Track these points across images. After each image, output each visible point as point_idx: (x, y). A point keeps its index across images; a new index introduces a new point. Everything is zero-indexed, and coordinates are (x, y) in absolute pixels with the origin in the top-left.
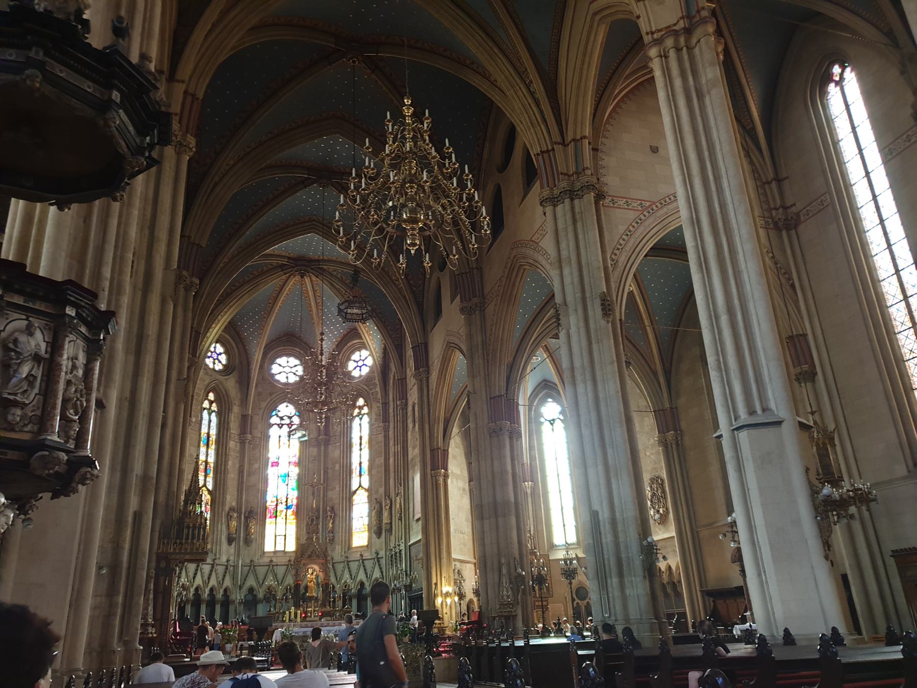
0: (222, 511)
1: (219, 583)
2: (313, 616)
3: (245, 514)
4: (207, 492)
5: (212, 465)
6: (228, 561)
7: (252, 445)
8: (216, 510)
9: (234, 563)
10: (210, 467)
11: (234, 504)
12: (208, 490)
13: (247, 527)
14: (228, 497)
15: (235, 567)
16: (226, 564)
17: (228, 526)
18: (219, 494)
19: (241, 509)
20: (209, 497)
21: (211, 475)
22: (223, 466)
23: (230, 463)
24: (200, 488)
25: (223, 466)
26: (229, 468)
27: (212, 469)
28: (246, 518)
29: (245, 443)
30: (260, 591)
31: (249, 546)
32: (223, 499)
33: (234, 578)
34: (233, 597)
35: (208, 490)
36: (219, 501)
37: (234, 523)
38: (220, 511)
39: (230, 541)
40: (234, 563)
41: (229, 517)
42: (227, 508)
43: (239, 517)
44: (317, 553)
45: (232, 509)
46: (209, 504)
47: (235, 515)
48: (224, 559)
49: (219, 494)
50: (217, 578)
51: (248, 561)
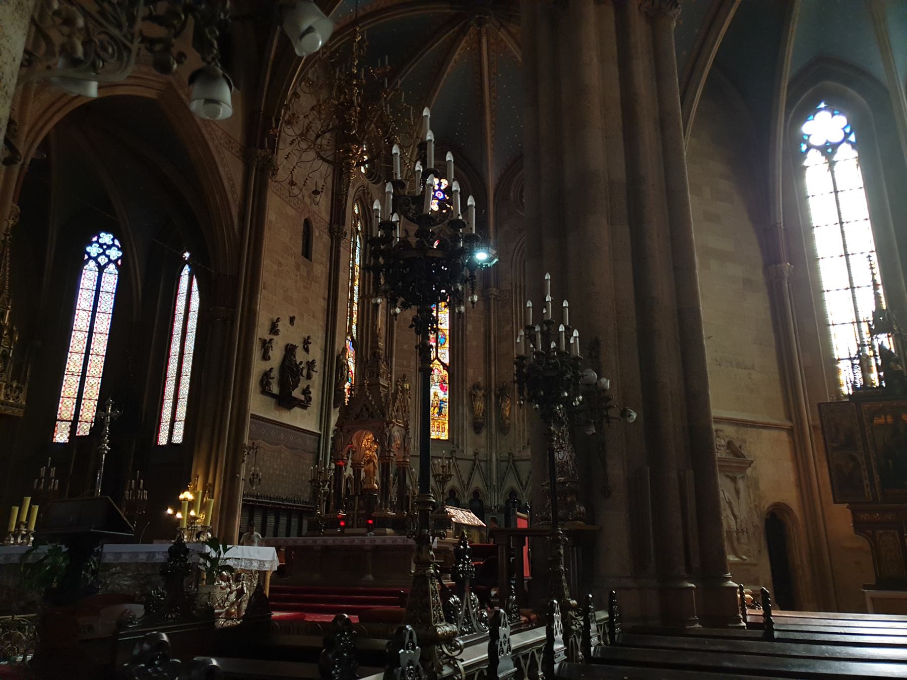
0: (463, 389)
1: (462, 482)
2: (355, 525)
3: (495, 391)
4: (441, 367)
5: (447, 333)
6: (476, 454)
7: (500, 302)
8: (456, 390)
9: (487, 457)
10: (444, 335)
11: (481, 379)
12: (442, 364)
13: (499, 408)
14: (470, 372)
15: (488, 461)
16: (473, 458)
17: (472, 409)
18: (458, 367)
19: (490, 385)
20: (445, 373)
21: (447, 345)
22: (460, 332)
23: (470, 327)
24: (431, 362)
25: (460, 332)
26: (468, 333)
27: (447, 337)
28: (497, 397)
29: (490, 299)
30: (524, 495)
31: (505, 434)
32: (463, 375)
33: (486, 478)
34: (487, 503)
35: (442, 364)
36: (458, 378)
37: (480, 405)
38: (460, 390)
39: (477, 428)
40: (487, 457)
41: (473, 397)
42: (469, 384)
43: (487, 397)
44: (371, 410)
45: (476, 386)
46: (447, 381)
47: (480, 393)
48: (469, 452)
49: (458, 367)
50: (459, 477)
51: (507, 455)
